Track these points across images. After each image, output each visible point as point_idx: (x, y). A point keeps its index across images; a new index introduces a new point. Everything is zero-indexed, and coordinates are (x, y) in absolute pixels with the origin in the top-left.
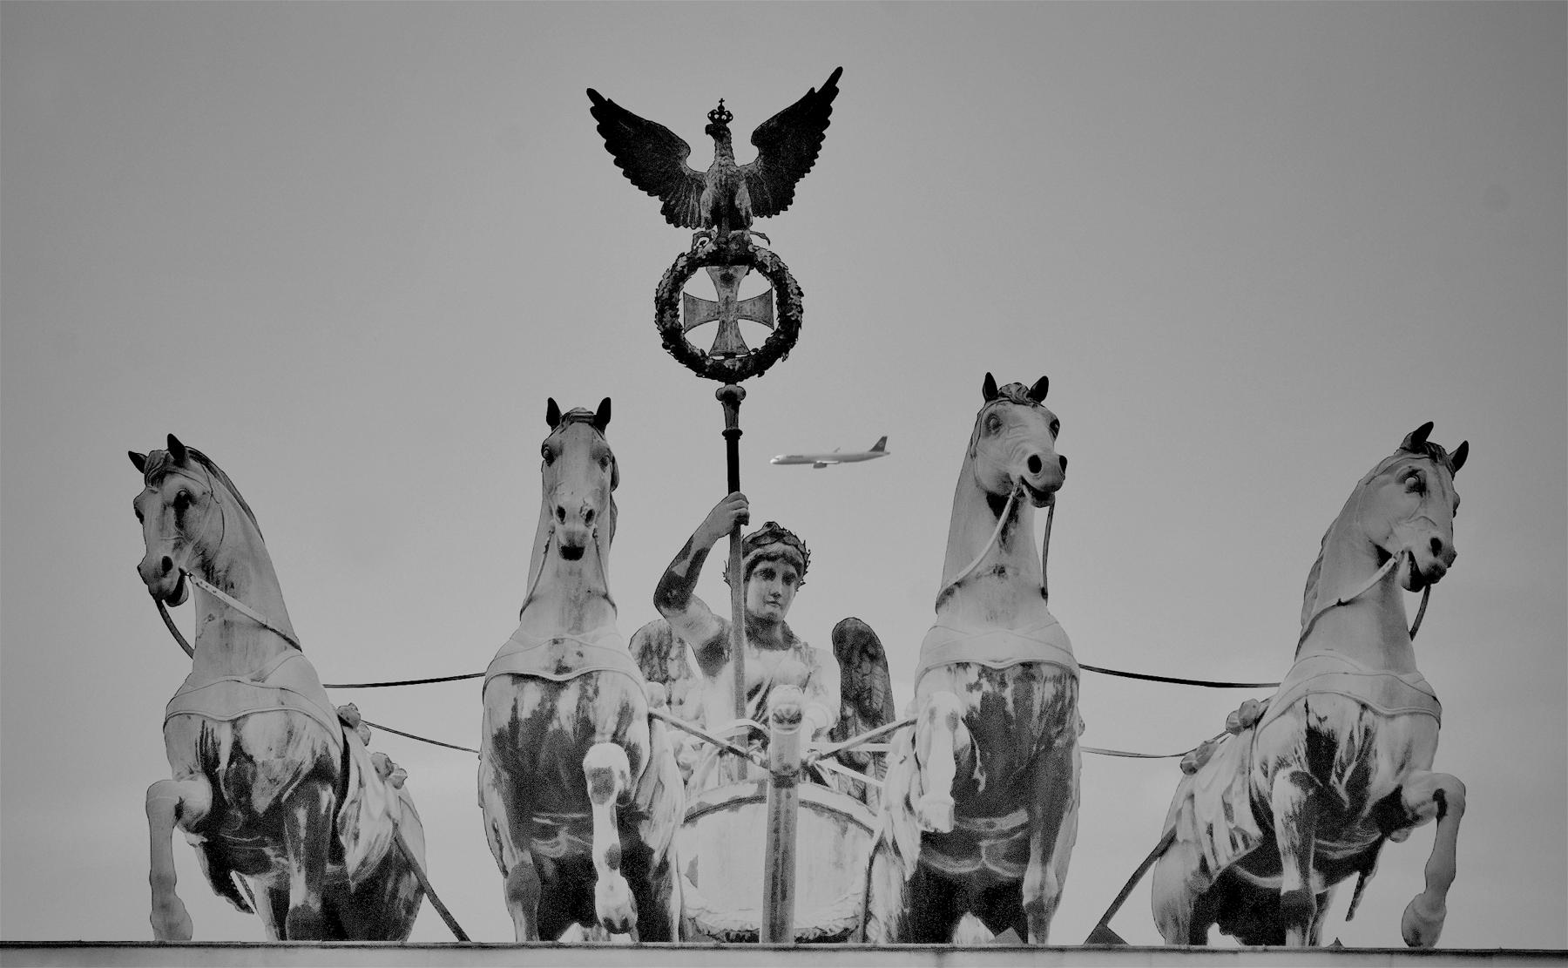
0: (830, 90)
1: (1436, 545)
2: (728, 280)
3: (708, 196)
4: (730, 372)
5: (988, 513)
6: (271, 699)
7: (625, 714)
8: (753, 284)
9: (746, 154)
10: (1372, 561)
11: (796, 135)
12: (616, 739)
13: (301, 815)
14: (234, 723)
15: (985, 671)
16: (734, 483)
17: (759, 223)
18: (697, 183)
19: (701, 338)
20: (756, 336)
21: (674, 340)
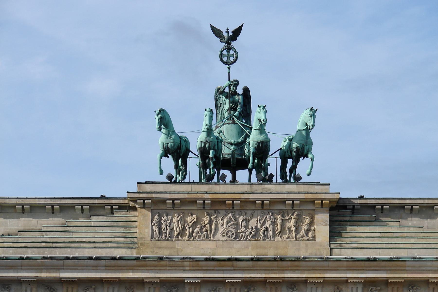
0: (242, 26)
1: (312, 125)
2: (228, 52)
3: (226, 40)
4: (229, 64)
5: (258, 121)
6: (172, 141)
7: (214, 146)
8: (232, 52)
9: (231, 34)
10: (305, 124)
11: (237, 32)
12: (213, 149)
13: (176, 154)
14: (168, 144)
15: (257, 142)
16: (229, 80)
17: (233, 43)
18: (224, 37)
19: (225, 59)
20: (232, 59)
21: (221, 60)
